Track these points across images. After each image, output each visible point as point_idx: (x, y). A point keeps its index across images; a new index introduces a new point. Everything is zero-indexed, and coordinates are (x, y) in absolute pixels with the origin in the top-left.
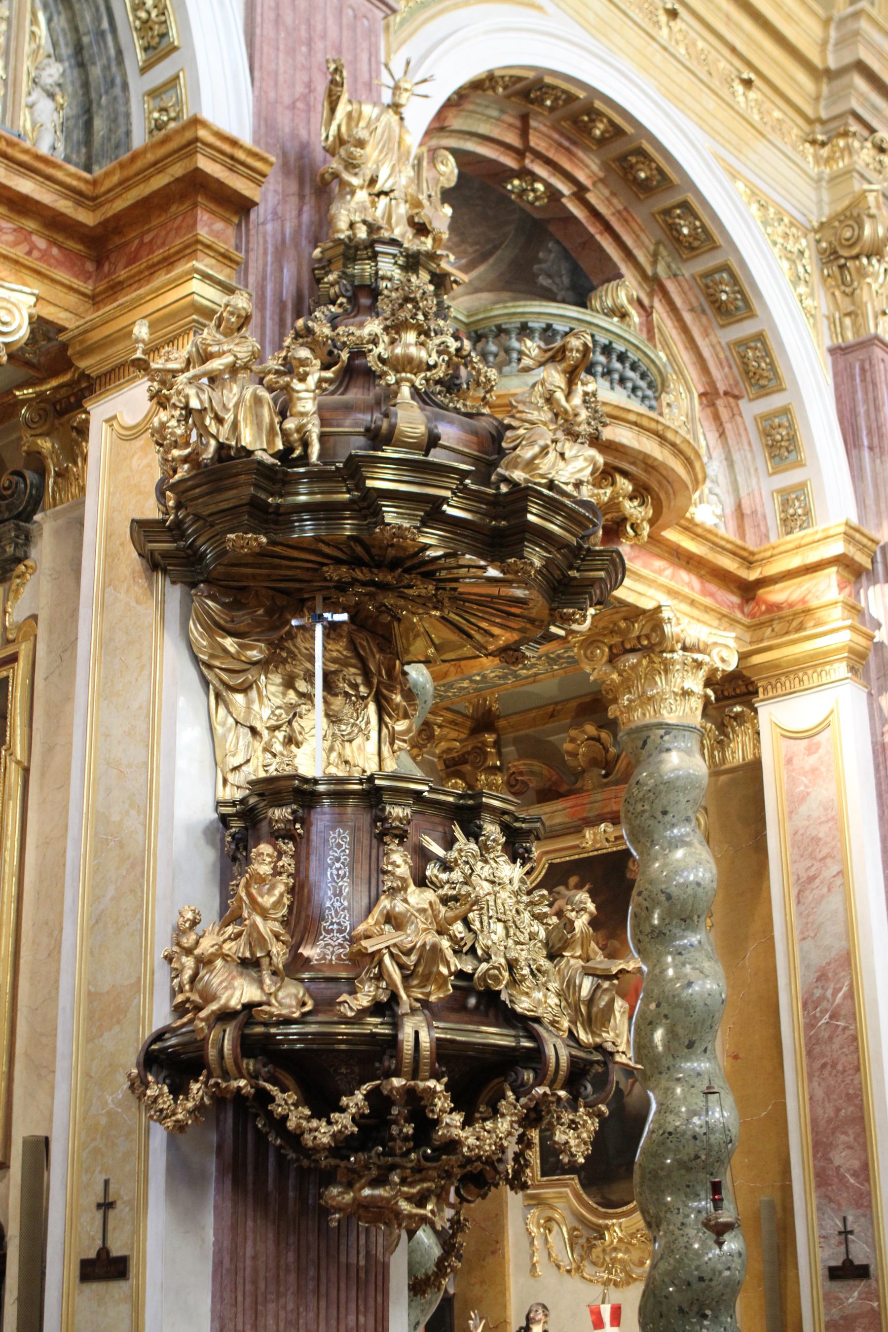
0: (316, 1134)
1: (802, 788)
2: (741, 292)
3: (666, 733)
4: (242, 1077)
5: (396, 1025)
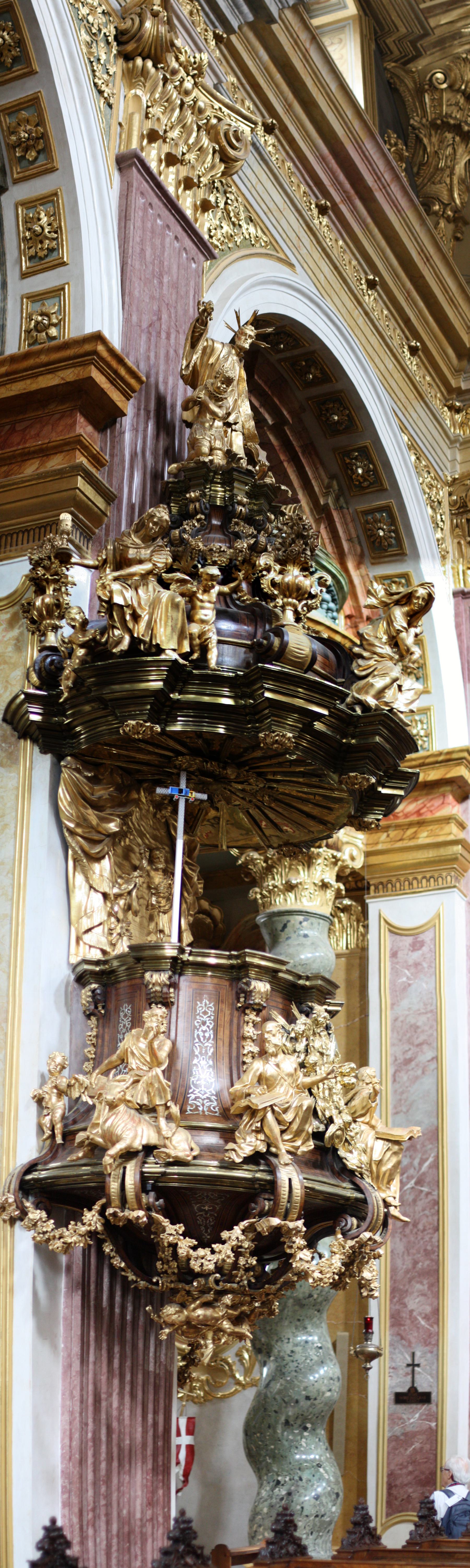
0: (203, 1261)
1: (404, 979)
2: (396, 531)
3: (305, 920)
4: (140, 1208)
5: (272, 1171)
